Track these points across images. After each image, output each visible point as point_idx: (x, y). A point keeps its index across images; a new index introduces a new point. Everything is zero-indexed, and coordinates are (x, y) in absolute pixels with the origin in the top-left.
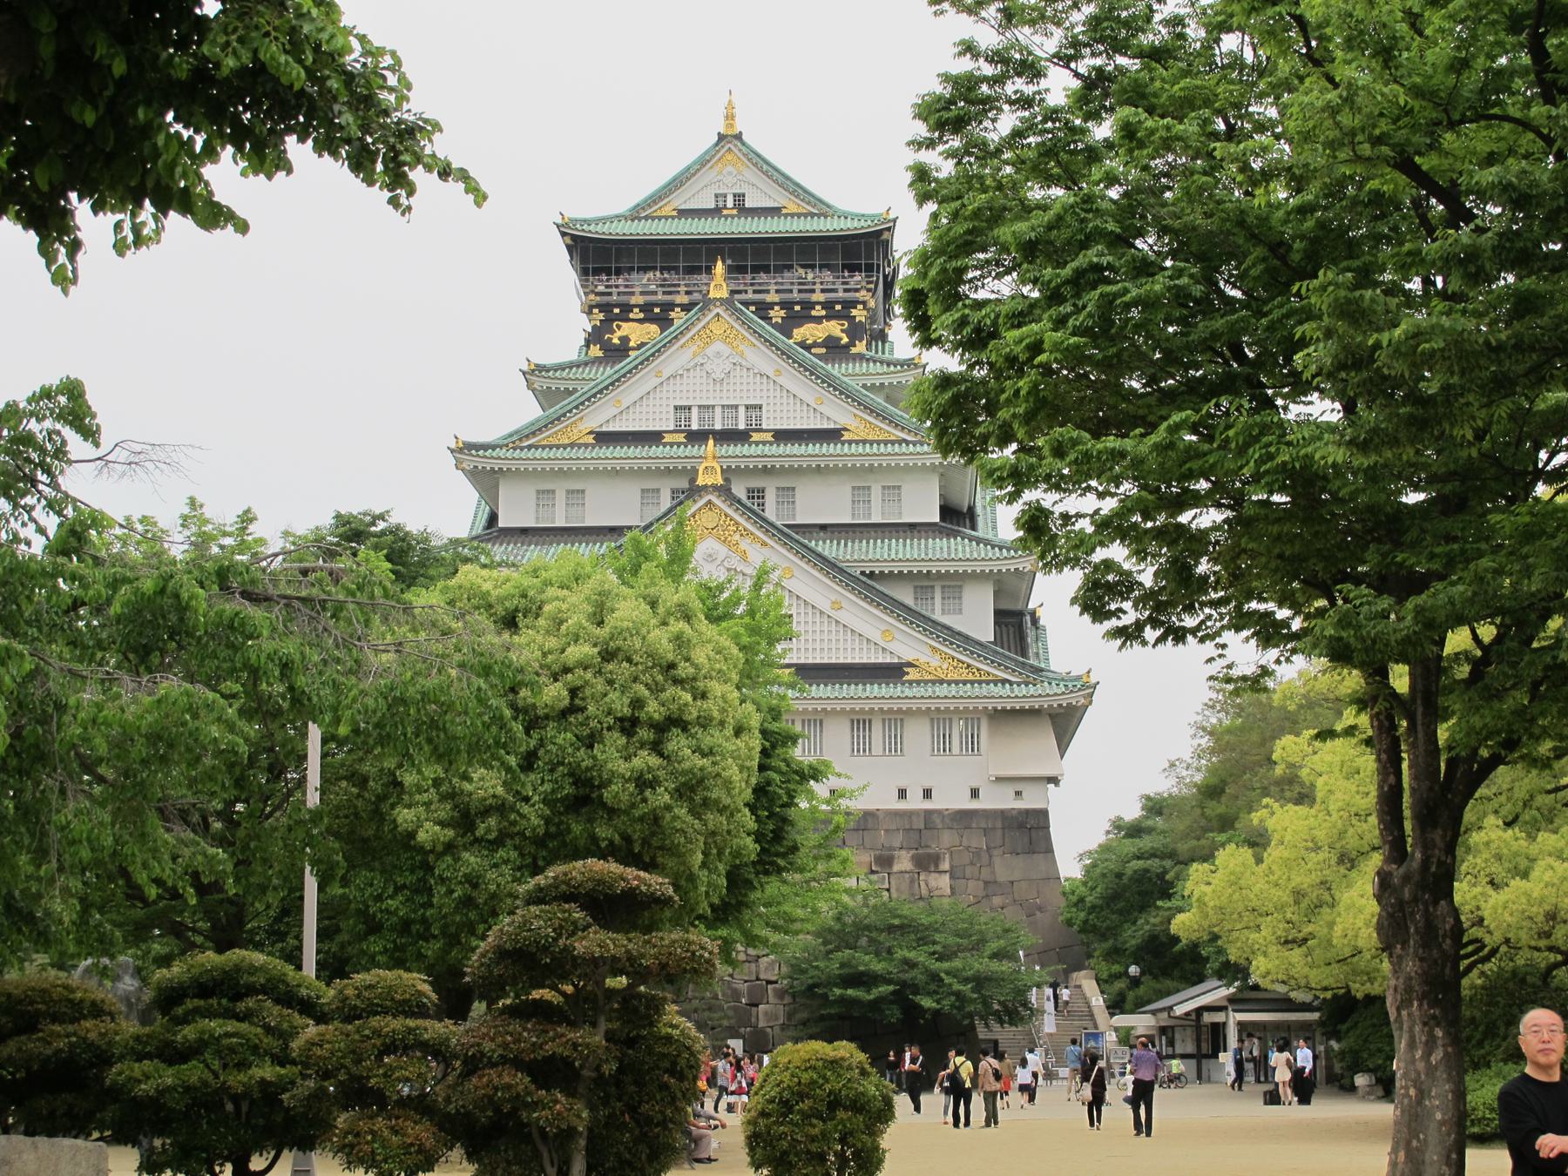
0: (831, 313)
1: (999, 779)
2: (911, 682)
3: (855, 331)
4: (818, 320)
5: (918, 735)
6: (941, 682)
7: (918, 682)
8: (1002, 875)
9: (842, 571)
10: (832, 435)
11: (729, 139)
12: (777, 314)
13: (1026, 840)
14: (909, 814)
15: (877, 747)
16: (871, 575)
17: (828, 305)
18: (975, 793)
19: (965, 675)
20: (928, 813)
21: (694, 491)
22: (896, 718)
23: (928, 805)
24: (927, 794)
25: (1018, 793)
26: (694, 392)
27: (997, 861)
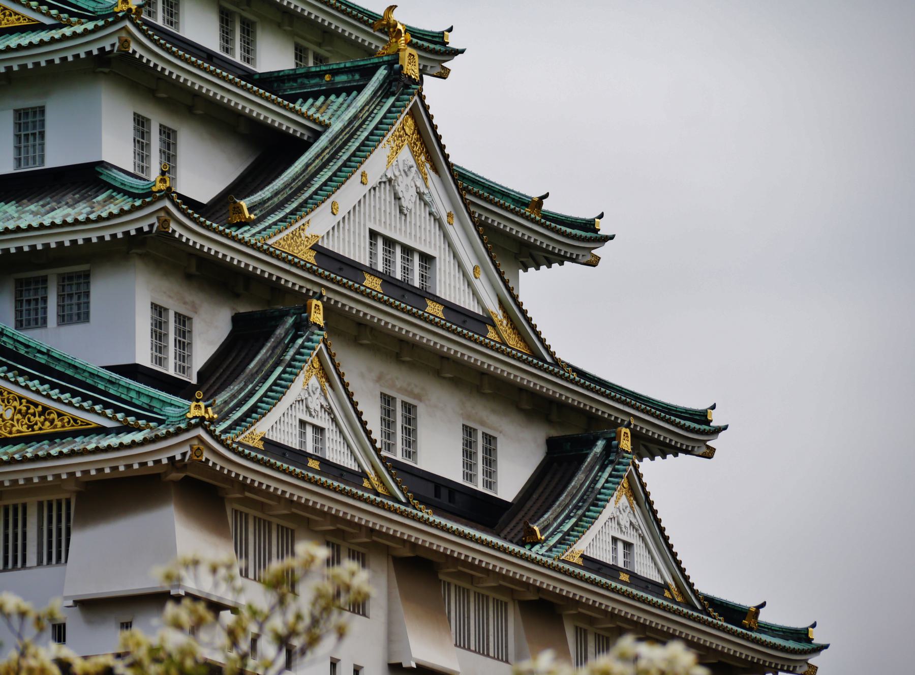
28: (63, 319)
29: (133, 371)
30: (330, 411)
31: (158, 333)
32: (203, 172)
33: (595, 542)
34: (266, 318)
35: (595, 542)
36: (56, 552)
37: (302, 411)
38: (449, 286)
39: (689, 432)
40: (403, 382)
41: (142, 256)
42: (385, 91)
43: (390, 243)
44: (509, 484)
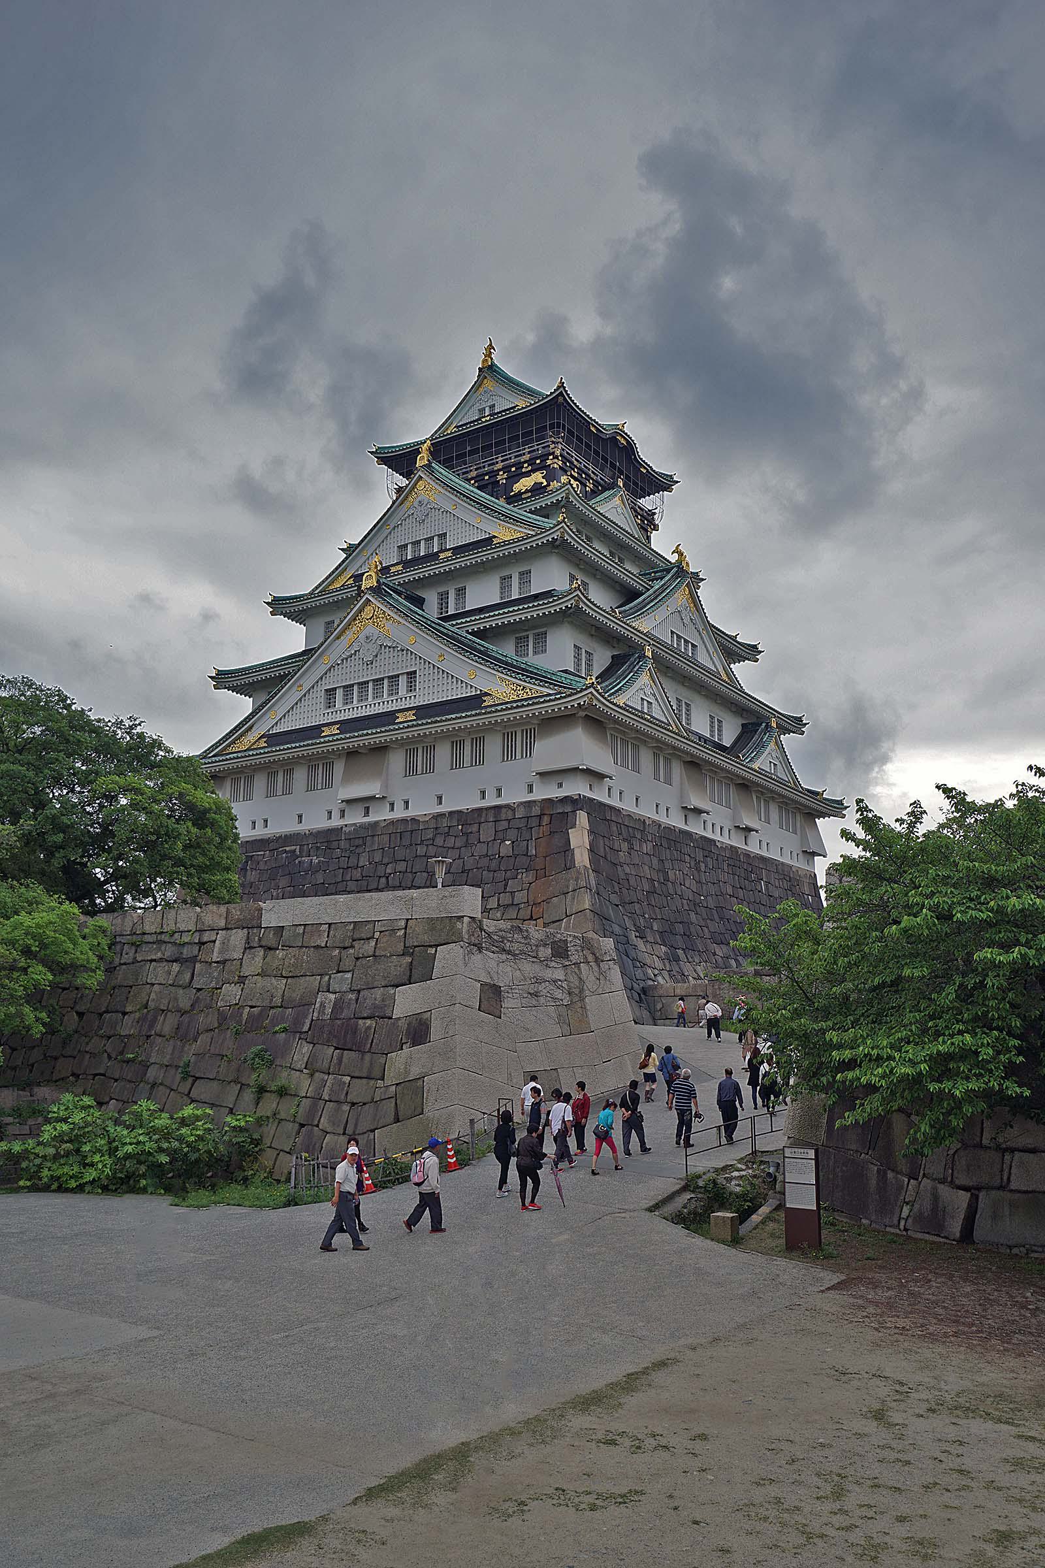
0: (535, 467)
1: (542, 774)
2: (486, 707)
3: (550, 477)
4: (528, 474)
5: (493, 746)
7: (491, 706)
10: (488, 541)
11: (489, 370)
12: (502, 478)
15: (467, 758)
16: (473, 633)
17: (531, 462)
20: (498, 808)
21: (360, 593)
23: (499, 802)
28: (535, 653)
29: (566, 671)
30: (654, 695)
31: (577, 657)
32: (600, 598)
33: (763, 762)
34: (625, 655)
35: (763, 762)
36: (528, 751)
37: (641, 693)
38: (703, 658)
39: (795, 725)
40: (686, 694)
41: (571, 623)
42: (676, 576)
43: (679, 637)
44: (727, 742)
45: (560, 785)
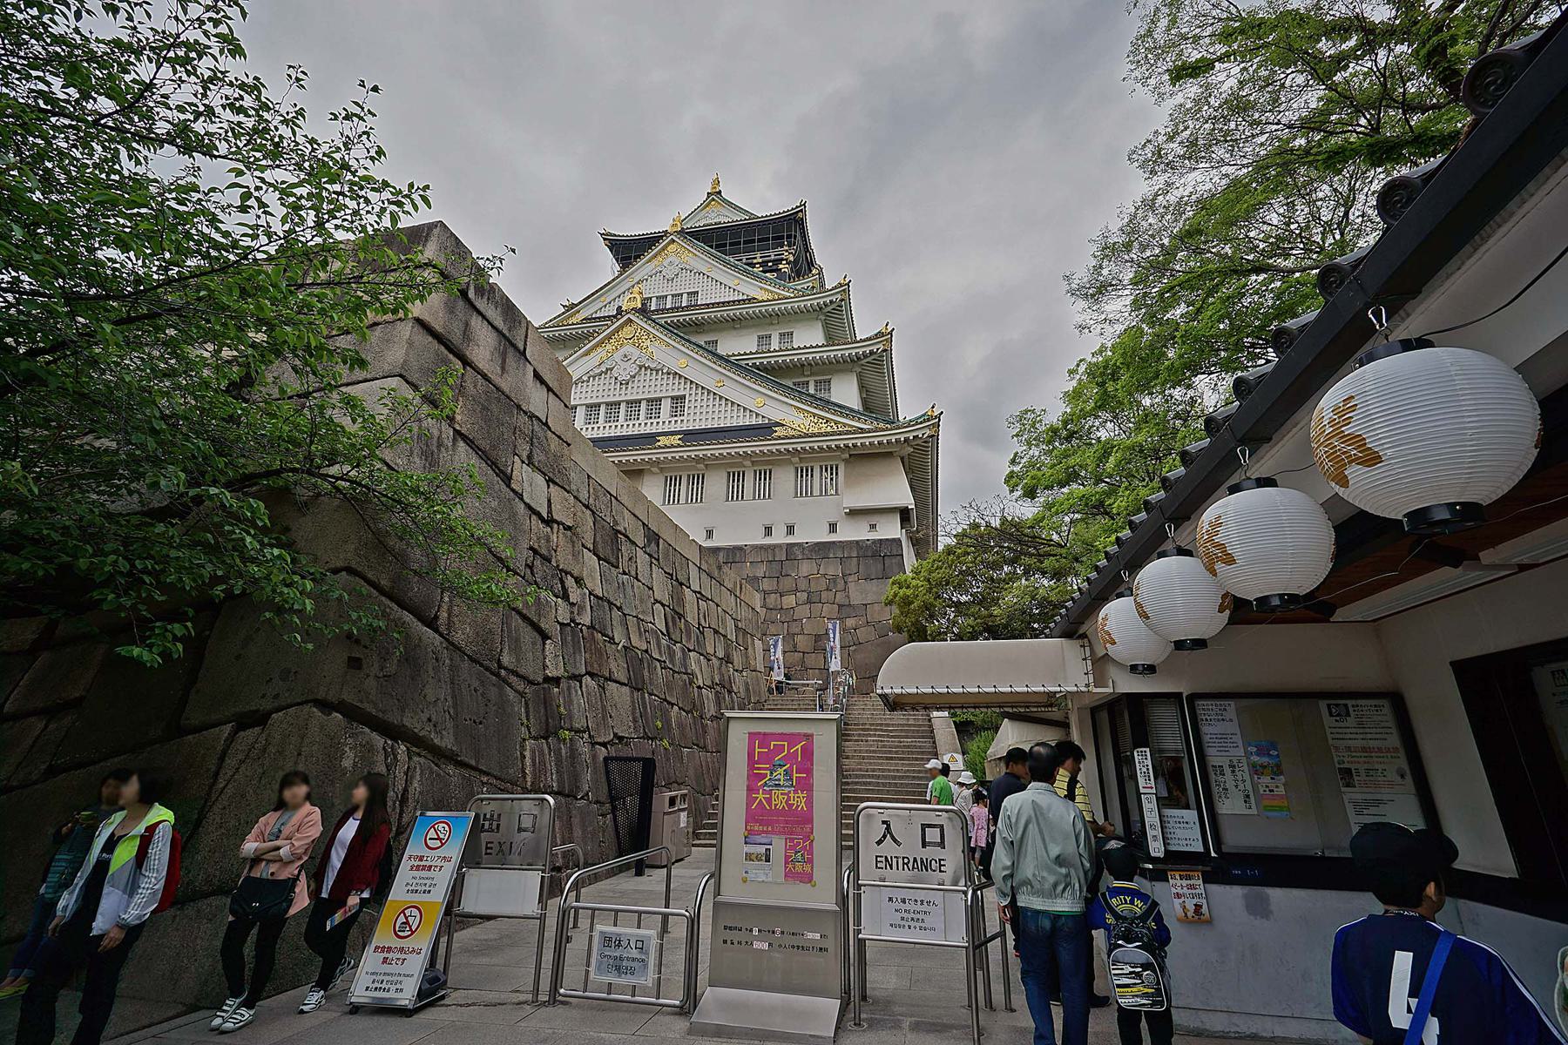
1: (854, 513)
5: (784, 479)
6: (807, 436)
8: (856, 599)
9: (727, 361)
13: (880, 566)
14: (773, 547)
17: (763, 264)
18: (833, 528)
19: (825, 428)
22: (765, 466)
23: (791, 540)
24: (790, 530)
25: (873, 527)
26: (653, 289)
27: (851, 586)
45: (873, 527)
